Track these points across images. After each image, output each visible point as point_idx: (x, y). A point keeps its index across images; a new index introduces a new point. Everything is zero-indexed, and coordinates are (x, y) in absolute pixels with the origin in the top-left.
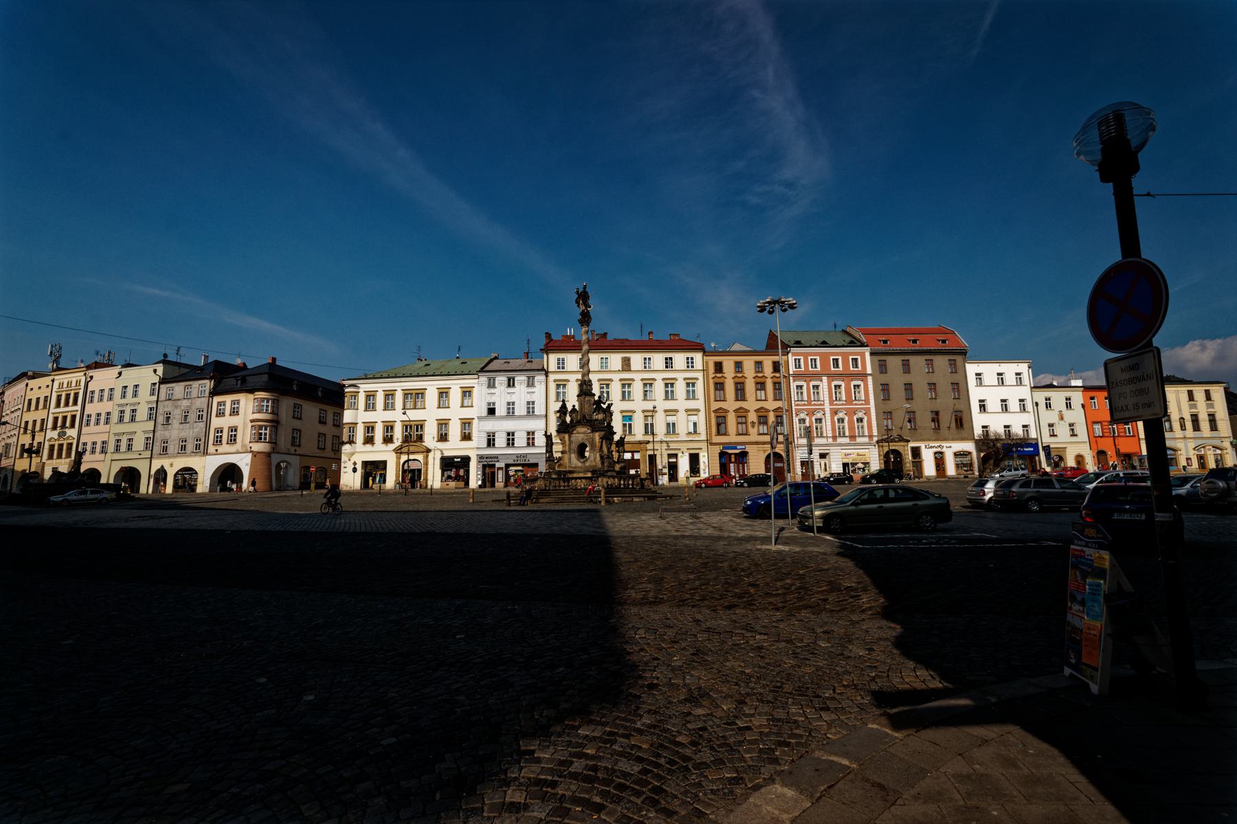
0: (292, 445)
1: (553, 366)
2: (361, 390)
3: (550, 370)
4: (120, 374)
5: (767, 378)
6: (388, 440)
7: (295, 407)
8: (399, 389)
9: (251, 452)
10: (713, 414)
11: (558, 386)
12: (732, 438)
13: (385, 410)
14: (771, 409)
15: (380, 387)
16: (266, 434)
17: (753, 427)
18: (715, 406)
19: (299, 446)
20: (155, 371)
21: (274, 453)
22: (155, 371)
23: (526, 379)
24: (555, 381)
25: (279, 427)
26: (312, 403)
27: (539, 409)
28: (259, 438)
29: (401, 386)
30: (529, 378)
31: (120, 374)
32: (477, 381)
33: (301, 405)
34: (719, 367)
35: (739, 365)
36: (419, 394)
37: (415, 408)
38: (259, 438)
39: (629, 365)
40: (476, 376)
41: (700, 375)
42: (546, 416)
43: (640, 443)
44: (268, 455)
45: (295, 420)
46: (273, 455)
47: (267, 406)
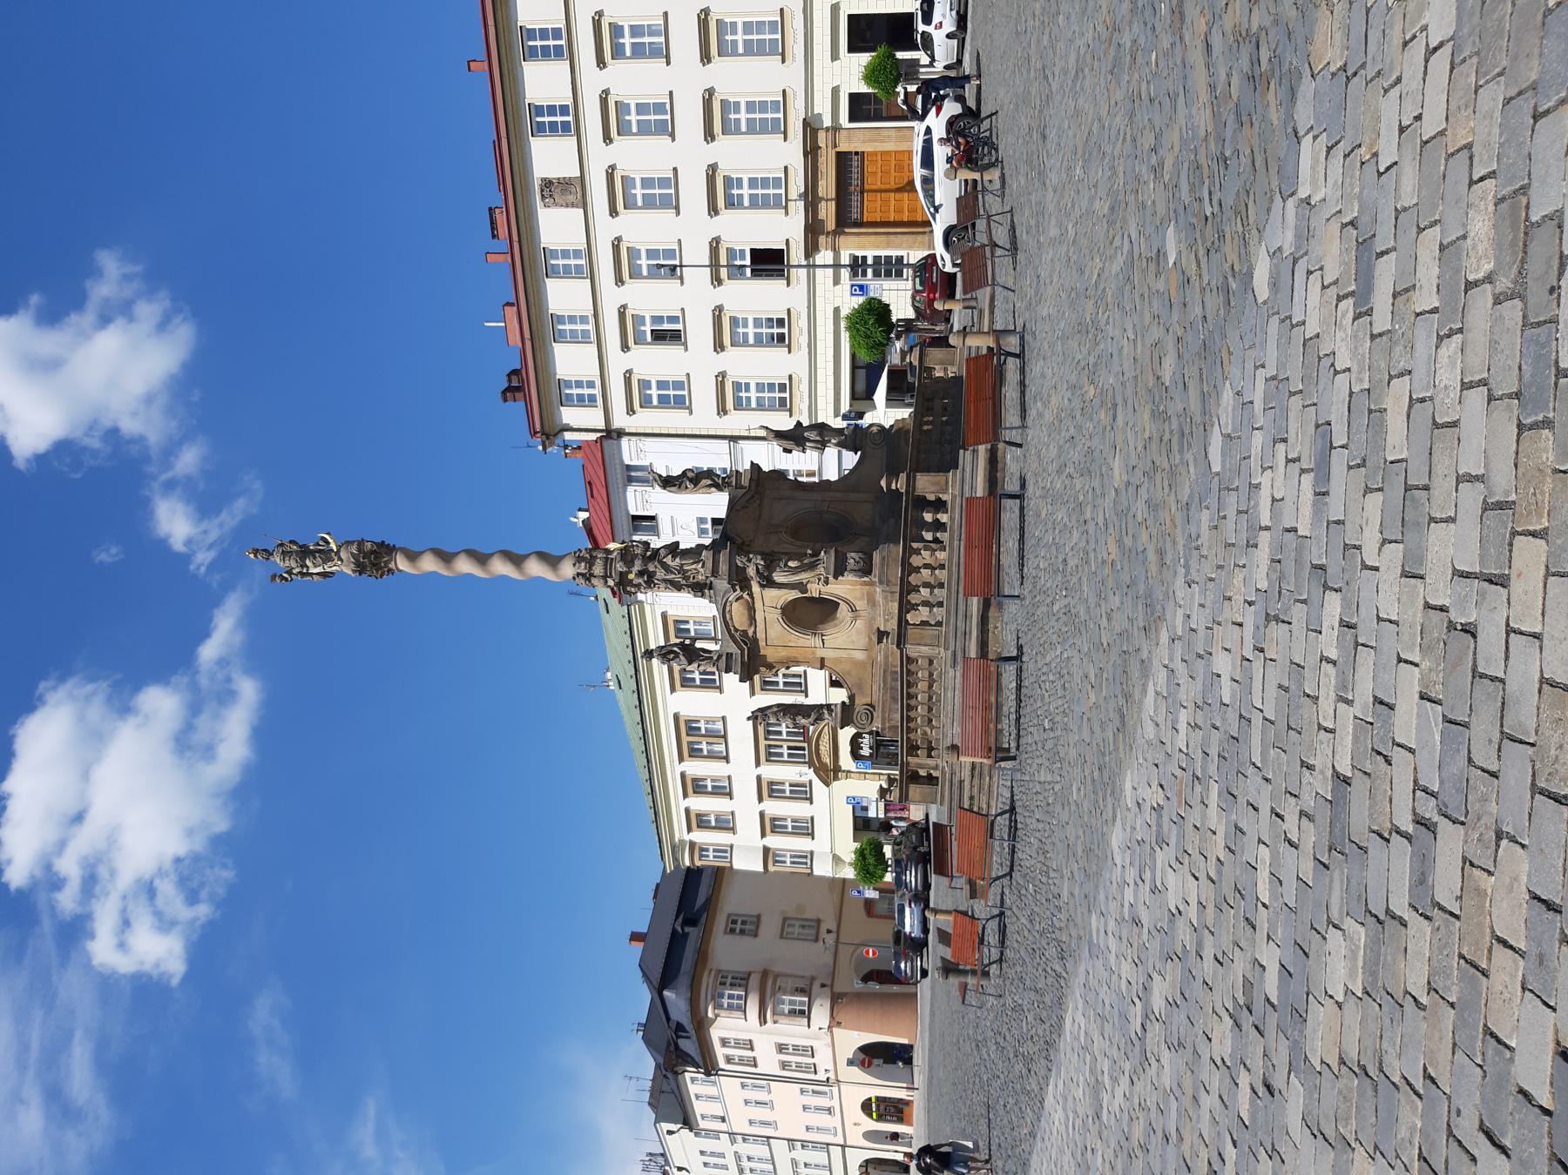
0: (816, 940)
1: (594, 418)
2: (687, 837)
4: (680, 1169)
6: (802, 793)
7: (733, 931)
8: (679, 768)
9: (830, 1027)
11: (646, 402)
13: (730, 795)
15: (679, 804)
16: (791, 1003)
19: (819, 921)
20: (670, 1132)
21: (832, 986)
22: (670, 1132)
23: (630, 489)
24: (631, 411)
25: (777, 968)
26: (724, 885)
28: (805, 1014)
29: (672, 762)
30: (630, 480)
31: (680, 1169)
32: (647, 608)
33: (729, 915)
36: (688, 728)
37: (725, 737)
38: (805, 1014)
39: (565, 184)
40: (635, 609)
42: (734, 439)
43: (811, 152)
44: (836, 999)
45: (763, 930)
46: (837, 989)
47: (731, 997)
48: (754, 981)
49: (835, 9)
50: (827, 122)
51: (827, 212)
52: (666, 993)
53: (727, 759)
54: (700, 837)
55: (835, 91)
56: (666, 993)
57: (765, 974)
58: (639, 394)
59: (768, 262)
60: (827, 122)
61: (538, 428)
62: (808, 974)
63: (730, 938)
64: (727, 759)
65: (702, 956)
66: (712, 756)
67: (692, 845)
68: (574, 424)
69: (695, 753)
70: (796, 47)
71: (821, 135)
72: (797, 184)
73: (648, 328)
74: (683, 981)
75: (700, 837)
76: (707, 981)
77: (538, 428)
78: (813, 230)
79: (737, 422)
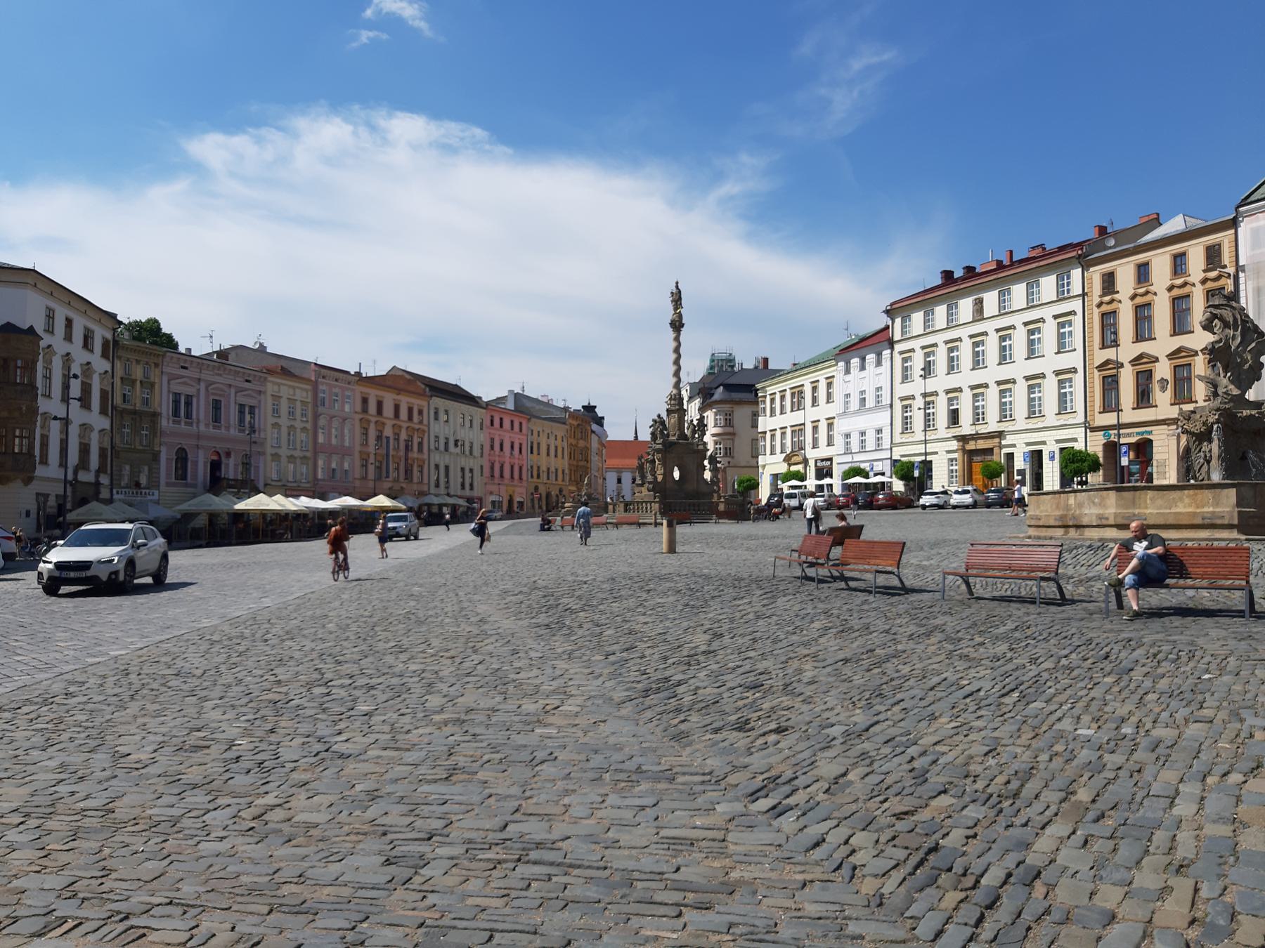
3: (895, 339)
5: (1194, 285)
10: (1097, 373)
12: (1129, 415)
14: (1199, 346)
17: (1163, 389)
18: (1101, 356)
24: (901, 353)
27: (886, 400)
32: (835, 368)
34: (1109, 282)
35: (1143, 272)
40: (833, 362)
41: (1076, 305)
42: (891, 406)
43: (991, 435)
48: (729, 430)
49: (1044, 443)
50: (1004, 442)
51: (971, 446)
52: (722, 388)
53: (792, 411)
54: (768, 400)
55: (1014, 446)
56: (722, 388)
57: (734, 434)
58: (907, 356)
59: (954, 417)
60: (1004, 442)
61: (894, 306)
62: (735, 455)
63: (750, 413)
64: (792, 411)
65: (740, 403)
66: (792, 403)
67: (765, 397)
68: (895, 325)
69: (793, 395)
70: (1032, 424)
71: (997, 440)
72: (982, 429)
73: (931, 358)
74: (727, 396)
75: (768, 400)
76: (727, 407)
77: (894, 306)
78: (963, 439)
79: (898, 405)
